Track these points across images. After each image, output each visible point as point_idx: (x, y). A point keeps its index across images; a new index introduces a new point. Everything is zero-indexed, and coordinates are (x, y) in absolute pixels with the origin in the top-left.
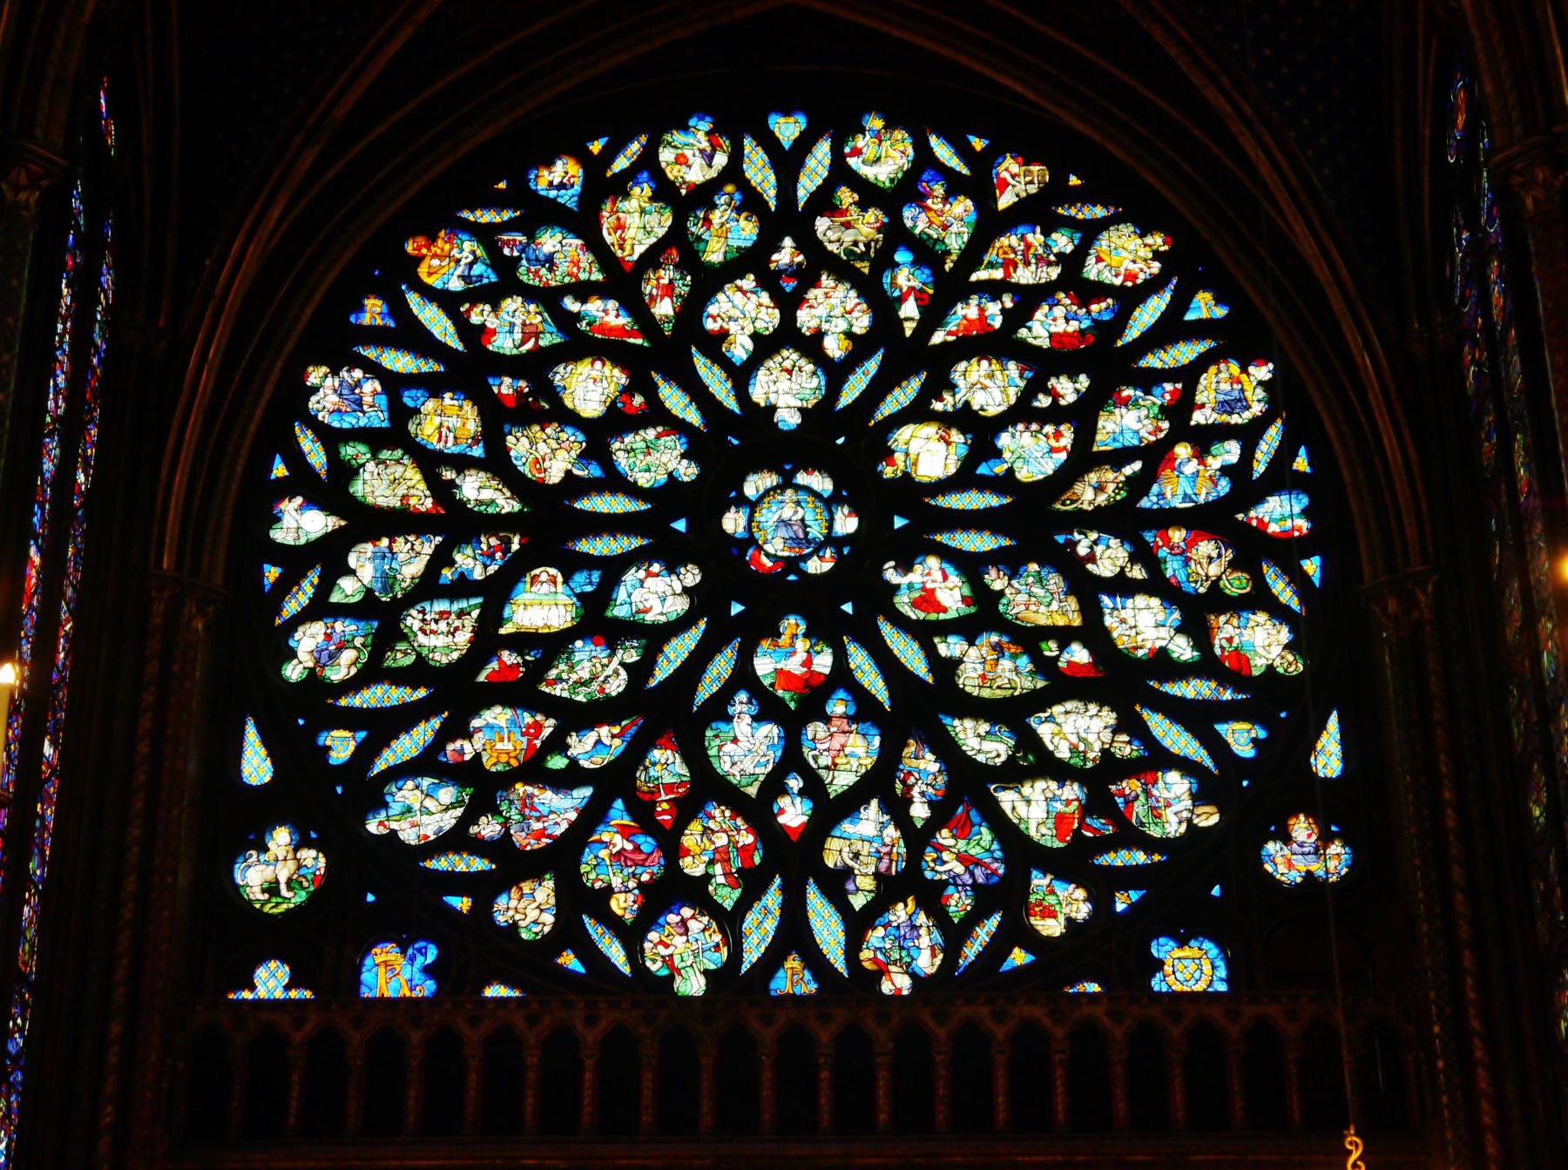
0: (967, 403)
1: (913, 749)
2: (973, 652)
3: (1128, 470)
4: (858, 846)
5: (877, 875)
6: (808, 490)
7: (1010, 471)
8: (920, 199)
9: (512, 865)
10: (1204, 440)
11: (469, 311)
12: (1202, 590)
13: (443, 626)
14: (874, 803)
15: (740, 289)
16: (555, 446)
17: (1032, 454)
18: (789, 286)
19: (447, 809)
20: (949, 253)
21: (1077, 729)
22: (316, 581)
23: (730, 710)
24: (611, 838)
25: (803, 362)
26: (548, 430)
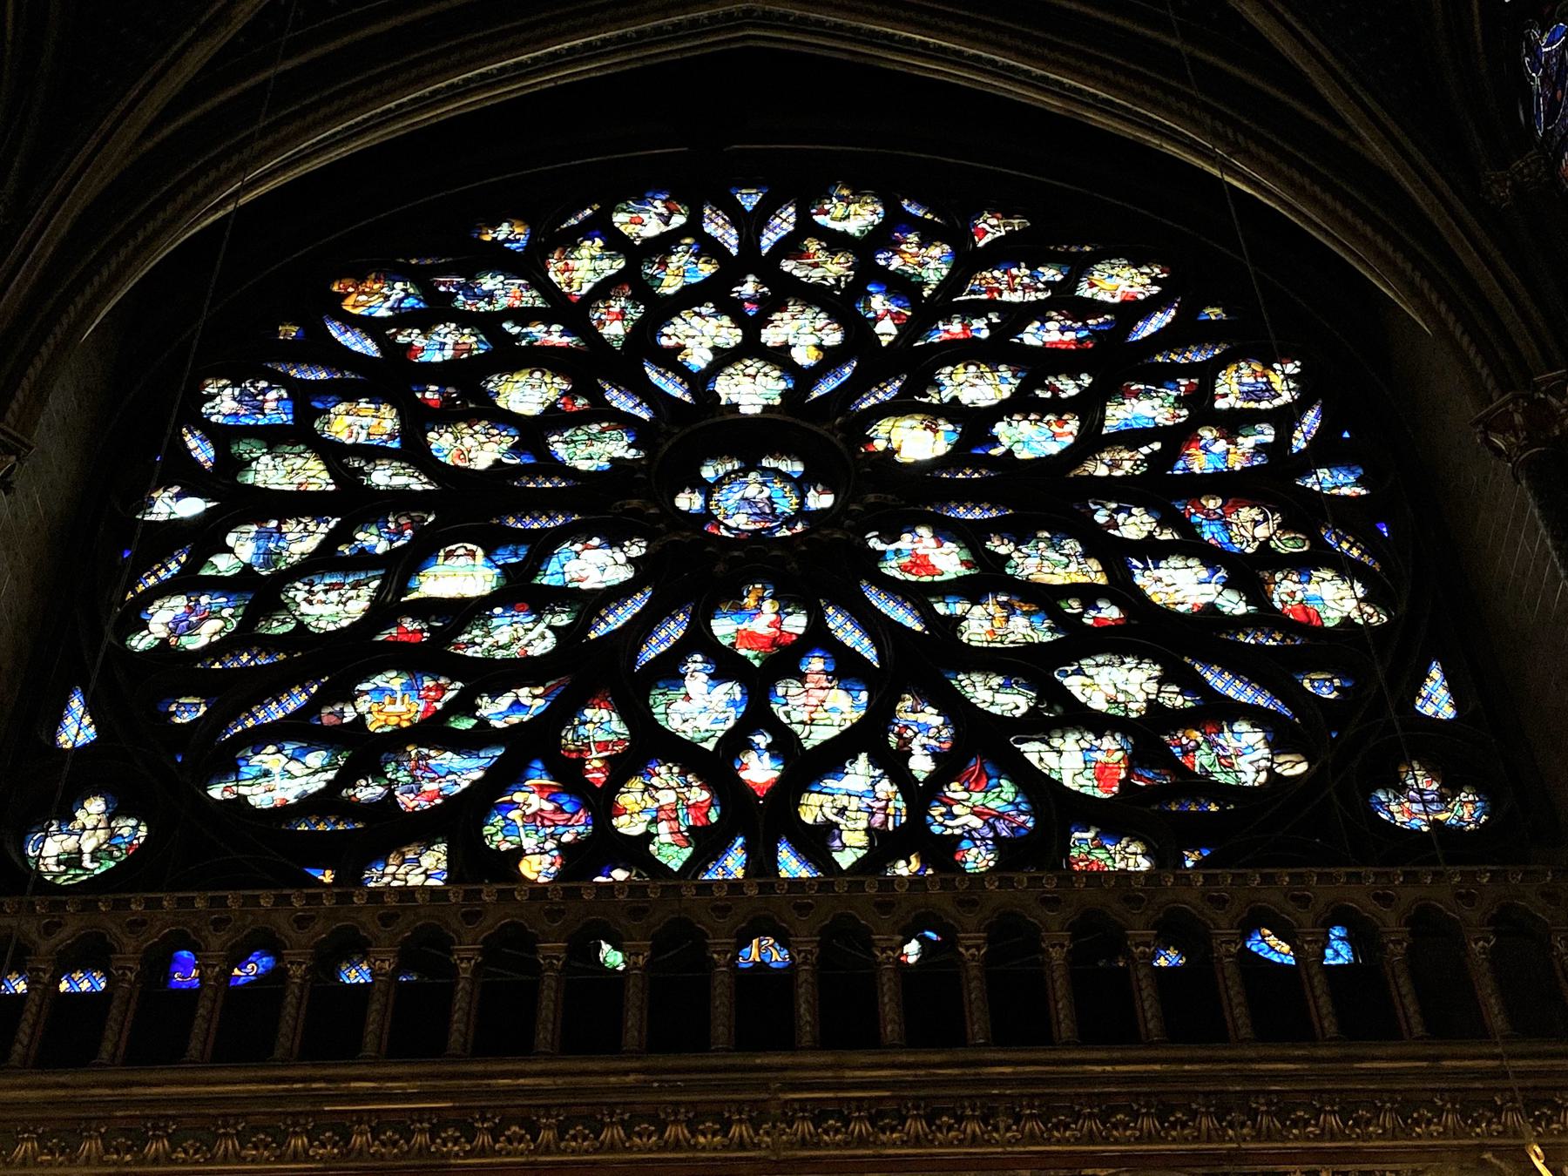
0: (955, 399)
1: (909, 703)
2: (978, 610)
3: (1145, 450)
4: (843, 801)
5: (869, 831)
6: (777, 471)
7: (1010, 452)
8: (894, 247)
9: (394, 829)
10: (1233, 424)
11: (394, 335)
12: (1249, 550)
13: (334, 596)
14: (863, 757)
15: (699, 314)
16: (482, 438)
17: (1030, 439)
18: (751, 310)
19: (316, 772)
20: (927, 284)
21: (1116, 683)
22: (183, 559)
23: (683, 670)
24: (530, 798)
25: (767, 369)
26: (477, 428)
